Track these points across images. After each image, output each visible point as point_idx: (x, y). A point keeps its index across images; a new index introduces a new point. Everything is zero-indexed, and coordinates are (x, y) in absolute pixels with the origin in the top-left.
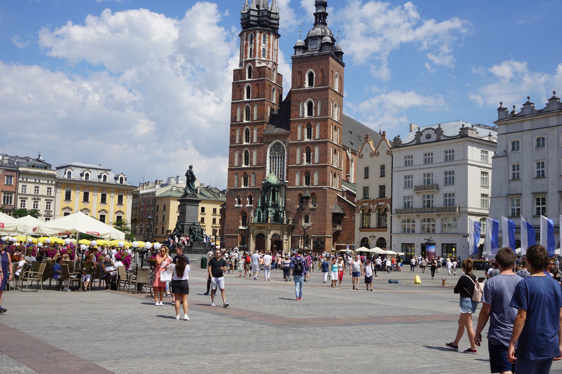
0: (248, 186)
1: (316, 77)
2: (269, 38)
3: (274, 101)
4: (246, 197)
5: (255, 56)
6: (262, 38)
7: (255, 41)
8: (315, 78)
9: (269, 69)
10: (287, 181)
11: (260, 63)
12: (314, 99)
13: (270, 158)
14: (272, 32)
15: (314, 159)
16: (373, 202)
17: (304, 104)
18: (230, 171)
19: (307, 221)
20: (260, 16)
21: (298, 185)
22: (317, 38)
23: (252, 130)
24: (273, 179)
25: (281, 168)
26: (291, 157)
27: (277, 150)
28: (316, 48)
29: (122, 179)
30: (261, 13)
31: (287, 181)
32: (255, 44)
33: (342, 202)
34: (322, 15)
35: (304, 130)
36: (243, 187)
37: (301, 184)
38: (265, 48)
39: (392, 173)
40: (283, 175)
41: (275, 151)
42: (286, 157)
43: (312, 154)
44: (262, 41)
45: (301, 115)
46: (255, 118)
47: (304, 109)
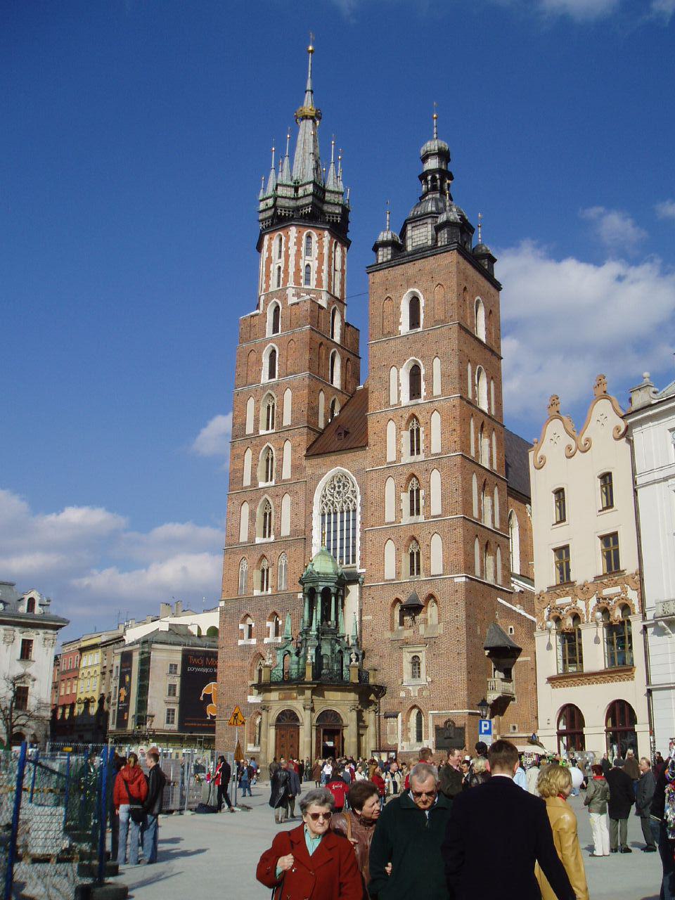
0: (270, 589)
1: (426, 305)
2: (320, 242)
3: (337, 383)
4: (265, 619)
5: (286, 282)
6: (304, 242)
7: (287, 249)
8: (423, 308)
9: (320, 307)
10: (364, 570)
11: (298, 295)
12: (422, 358)
13: (323, 515)
14: (328, 230)
15: (429, 506)
16: (585, 590)
17: (398, 371)
18: (228, 556)
19: (416, 673)
20: (301, 197)
21: (394, 577)
22: (425, 221)
23: (281, 449)
24: (323, 565)
25: (348, 538)
26: (373, 504)
27: (339, 493)
28: (426, 241)
29: (31, 601)
30: (301, 192)
31: (364, 570)
32: (287, 256)
33: (512, 618)
34: (438, 176)
35: (402, 436)
36: (257, 592)
37: (398, 574)
38: (311, 264)
39: (635, 491)
40: (354, 556)
41: (332, 495)
42: (359, 509)
43: (422, 493)
44: (303, 249)
45: (393, 400)
46: (287, 421)
47: (399, 385)
